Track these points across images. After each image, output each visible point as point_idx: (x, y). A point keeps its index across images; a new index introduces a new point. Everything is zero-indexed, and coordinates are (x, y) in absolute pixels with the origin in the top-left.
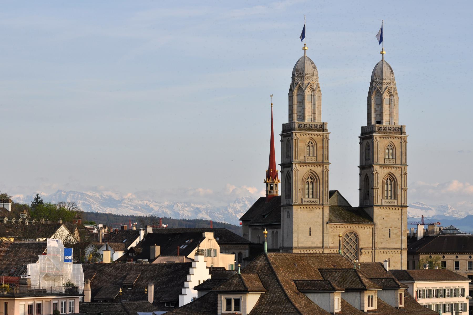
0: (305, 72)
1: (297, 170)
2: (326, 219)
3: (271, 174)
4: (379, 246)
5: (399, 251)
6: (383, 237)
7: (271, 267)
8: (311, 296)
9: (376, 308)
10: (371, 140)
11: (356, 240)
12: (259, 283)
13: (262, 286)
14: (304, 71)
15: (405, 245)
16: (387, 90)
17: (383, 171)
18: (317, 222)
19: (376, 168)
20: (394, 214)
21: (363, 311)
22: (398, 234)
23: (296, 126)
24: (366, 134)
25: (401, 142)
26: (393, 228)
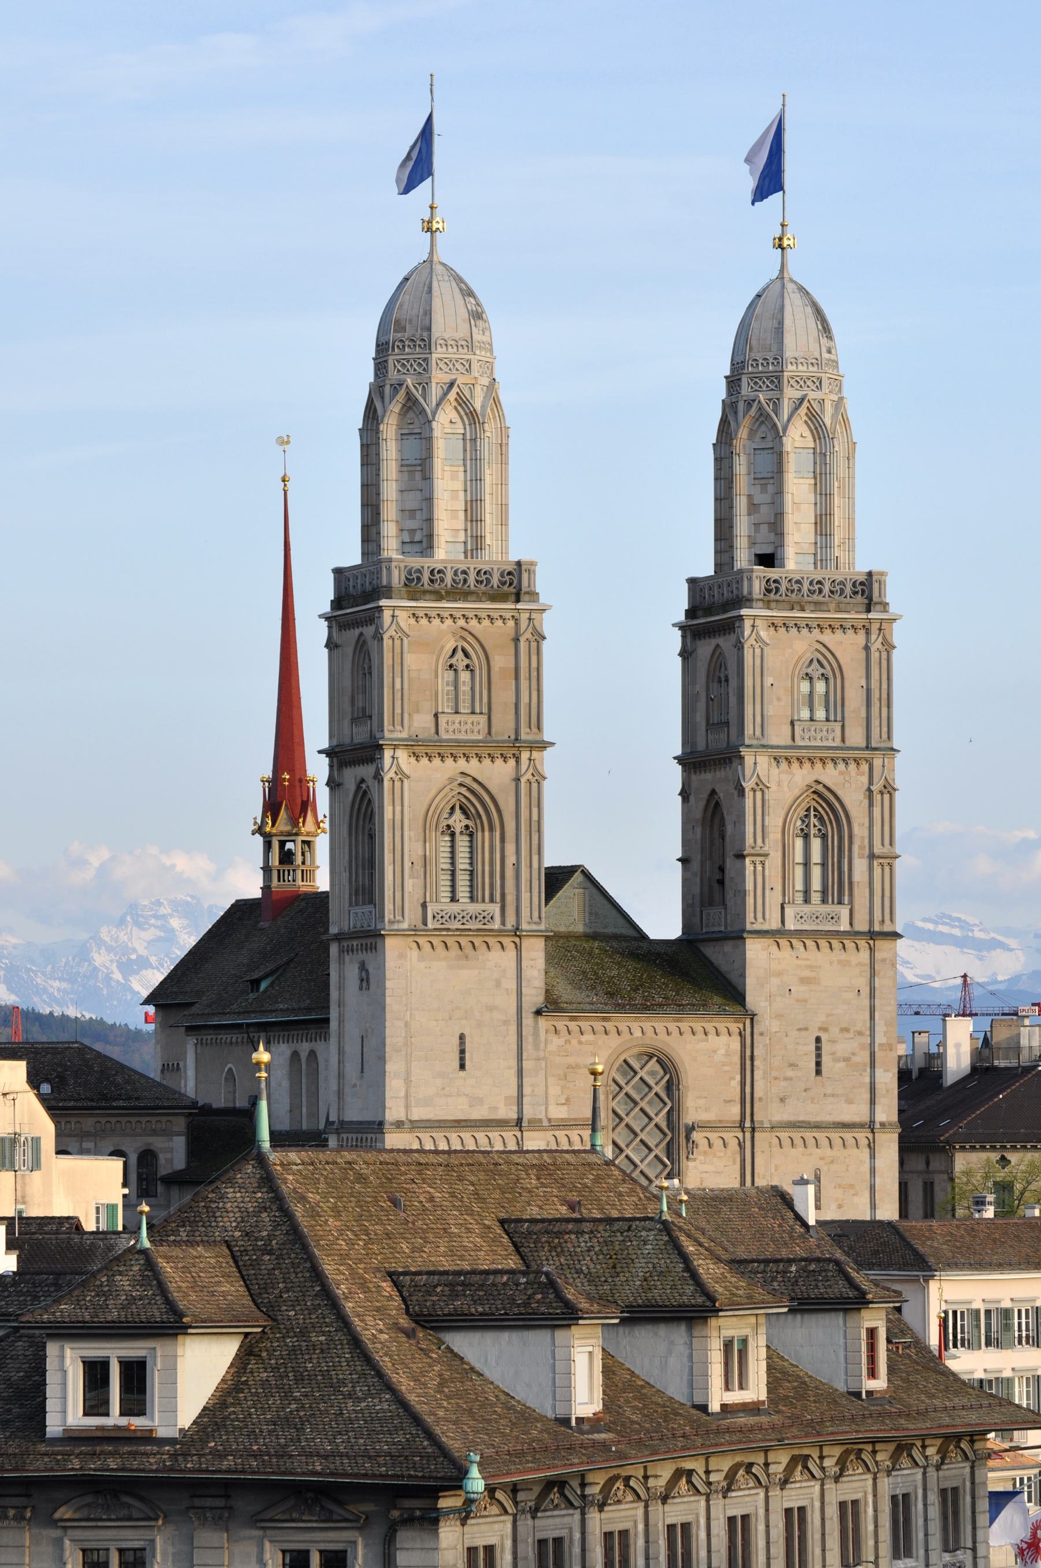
0: (437, 331)
1: (402, 776)
2: (534, 996)
4: (768, 1112)
5: (862, 1136)
6: (790, 1073)
7: (287, 1214)
8: (466, 1344)
9: (763, 1396)
10: (732, 638)
11: (669, 1087)
12: (232, 1289)
13: (247, 1301)
14: (429, 329)
15: (888, 1110)
16: (803, 411)
17: (785, 777)
18: (491, 1009)
19: (756, 765)
20: (840, 970)
21: (704, 1408)
22: (856, 1059)
23: (397, 579)
24: (709, 611)
25: (867, 648)
26: (835, 1031)
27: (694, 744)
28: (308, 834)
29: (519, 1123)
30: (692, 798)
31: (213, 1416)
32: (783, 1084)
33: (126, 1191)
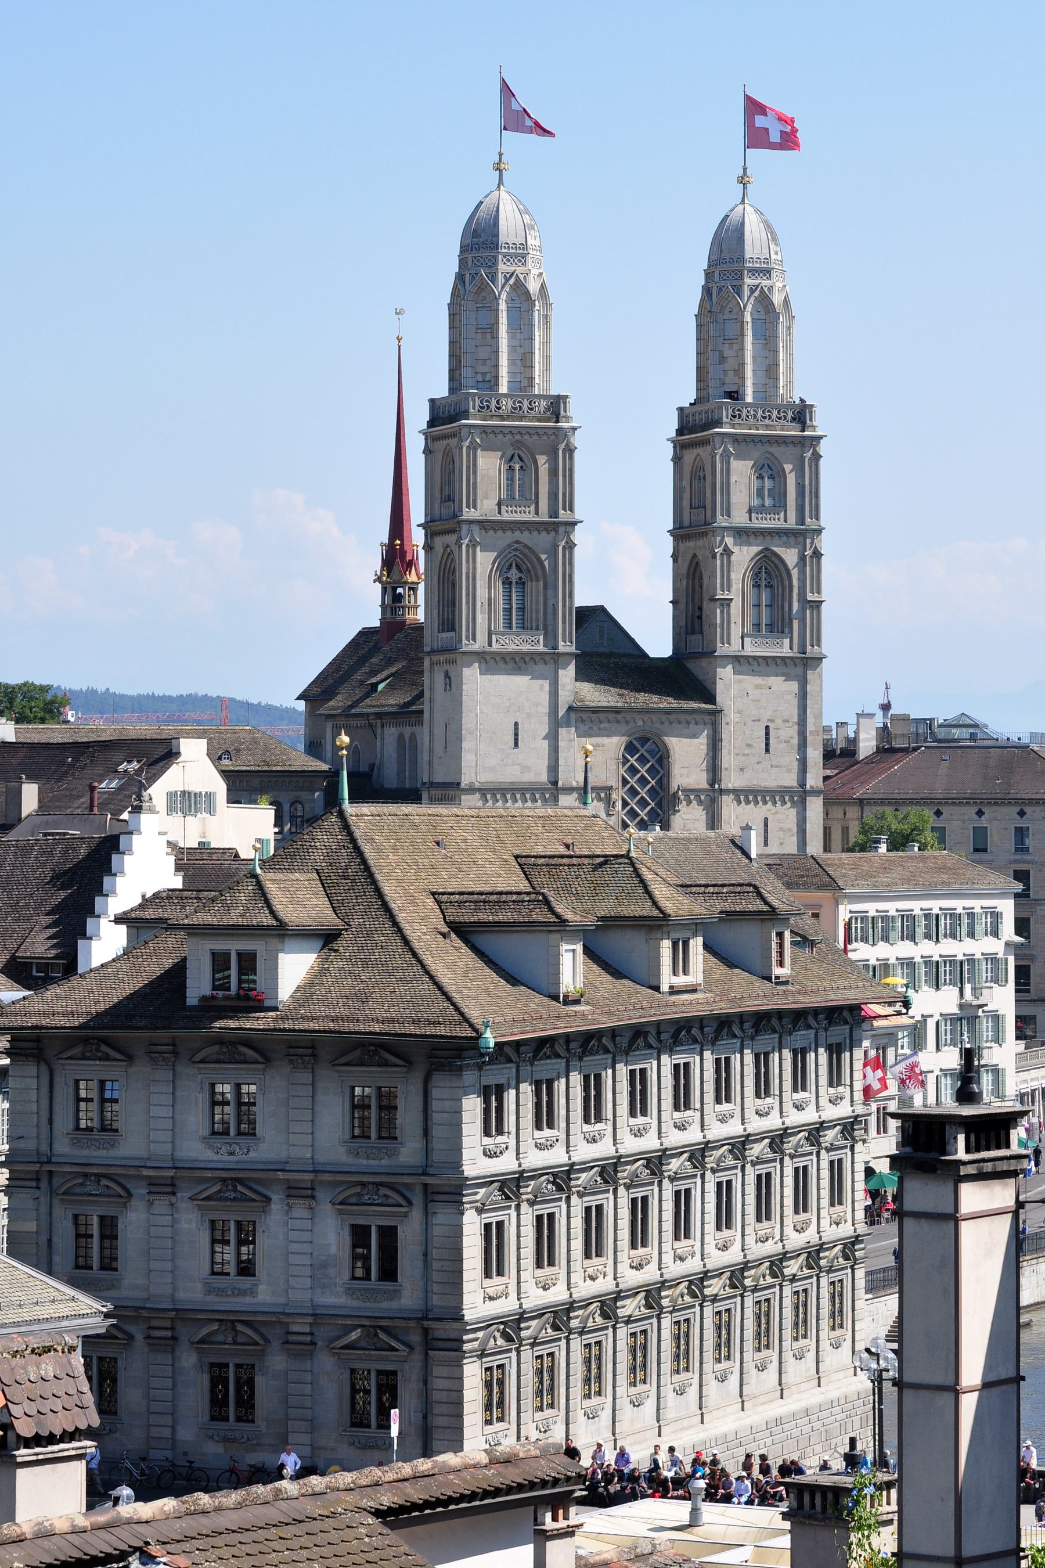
3: (395, 558)
4: (731, 780)
6: (747, 751)
9: (700, 980)
10: (709, 448)
13: (330, 912)
26: (779, 722)
27: (681, 522)
28: (412, 583)
29: (555, 783)
30: (680, 559)
31: (306, 992)
32: (743, 758)
33: (277, 830)
